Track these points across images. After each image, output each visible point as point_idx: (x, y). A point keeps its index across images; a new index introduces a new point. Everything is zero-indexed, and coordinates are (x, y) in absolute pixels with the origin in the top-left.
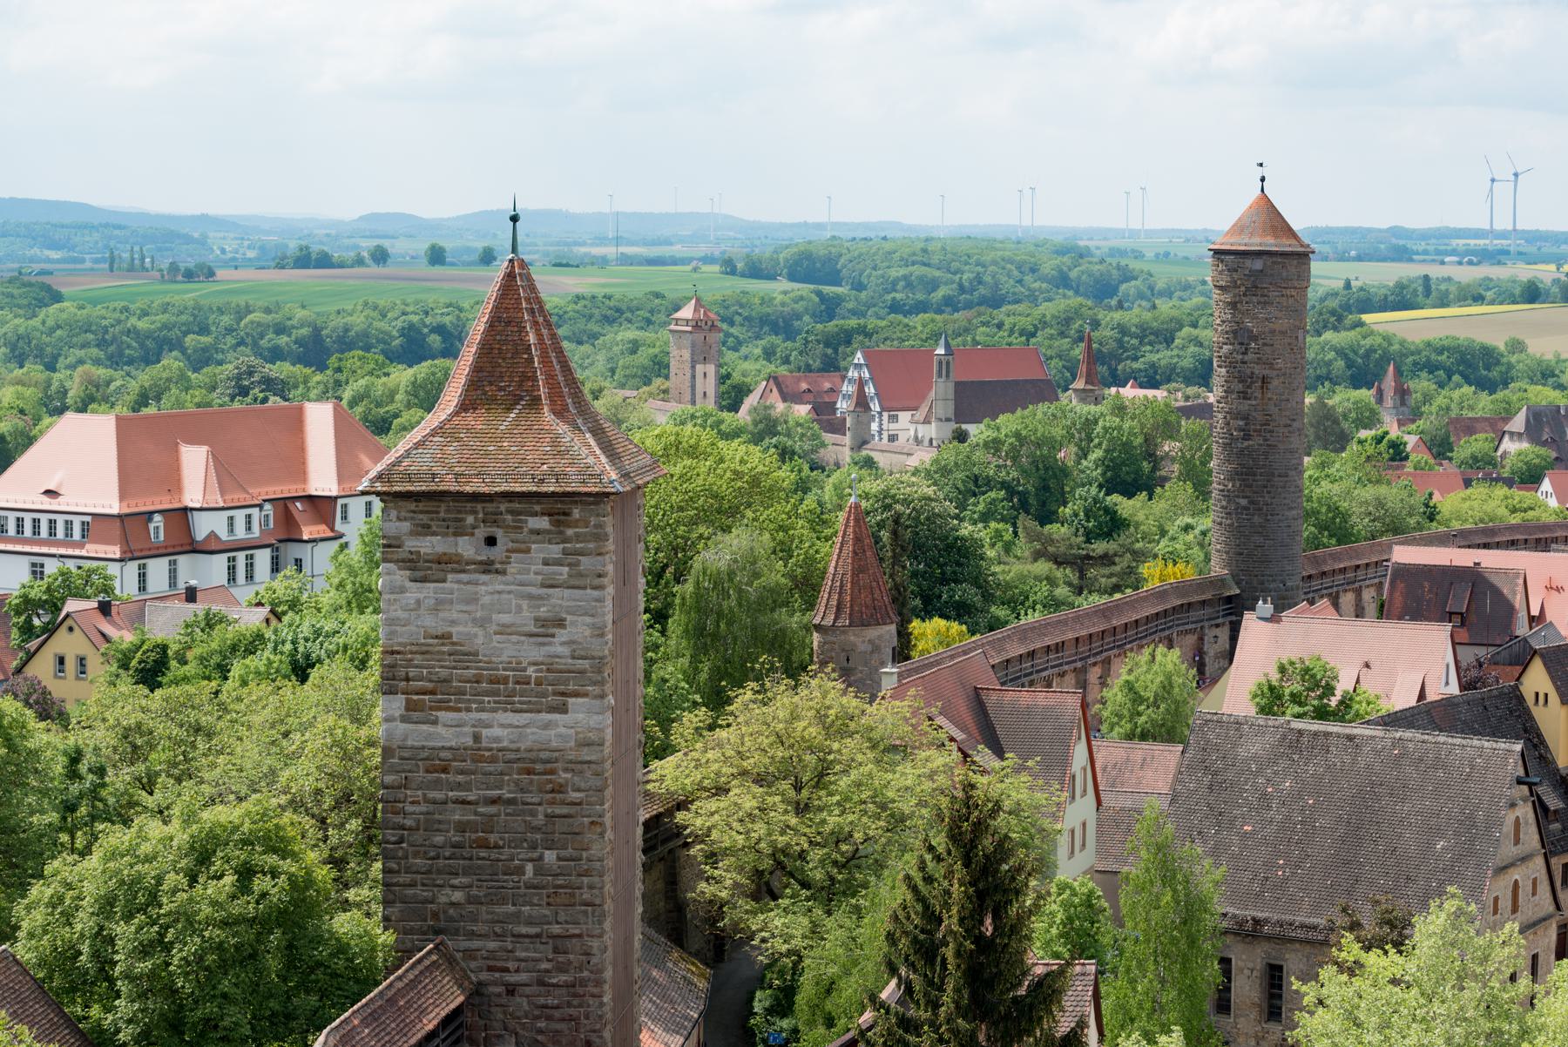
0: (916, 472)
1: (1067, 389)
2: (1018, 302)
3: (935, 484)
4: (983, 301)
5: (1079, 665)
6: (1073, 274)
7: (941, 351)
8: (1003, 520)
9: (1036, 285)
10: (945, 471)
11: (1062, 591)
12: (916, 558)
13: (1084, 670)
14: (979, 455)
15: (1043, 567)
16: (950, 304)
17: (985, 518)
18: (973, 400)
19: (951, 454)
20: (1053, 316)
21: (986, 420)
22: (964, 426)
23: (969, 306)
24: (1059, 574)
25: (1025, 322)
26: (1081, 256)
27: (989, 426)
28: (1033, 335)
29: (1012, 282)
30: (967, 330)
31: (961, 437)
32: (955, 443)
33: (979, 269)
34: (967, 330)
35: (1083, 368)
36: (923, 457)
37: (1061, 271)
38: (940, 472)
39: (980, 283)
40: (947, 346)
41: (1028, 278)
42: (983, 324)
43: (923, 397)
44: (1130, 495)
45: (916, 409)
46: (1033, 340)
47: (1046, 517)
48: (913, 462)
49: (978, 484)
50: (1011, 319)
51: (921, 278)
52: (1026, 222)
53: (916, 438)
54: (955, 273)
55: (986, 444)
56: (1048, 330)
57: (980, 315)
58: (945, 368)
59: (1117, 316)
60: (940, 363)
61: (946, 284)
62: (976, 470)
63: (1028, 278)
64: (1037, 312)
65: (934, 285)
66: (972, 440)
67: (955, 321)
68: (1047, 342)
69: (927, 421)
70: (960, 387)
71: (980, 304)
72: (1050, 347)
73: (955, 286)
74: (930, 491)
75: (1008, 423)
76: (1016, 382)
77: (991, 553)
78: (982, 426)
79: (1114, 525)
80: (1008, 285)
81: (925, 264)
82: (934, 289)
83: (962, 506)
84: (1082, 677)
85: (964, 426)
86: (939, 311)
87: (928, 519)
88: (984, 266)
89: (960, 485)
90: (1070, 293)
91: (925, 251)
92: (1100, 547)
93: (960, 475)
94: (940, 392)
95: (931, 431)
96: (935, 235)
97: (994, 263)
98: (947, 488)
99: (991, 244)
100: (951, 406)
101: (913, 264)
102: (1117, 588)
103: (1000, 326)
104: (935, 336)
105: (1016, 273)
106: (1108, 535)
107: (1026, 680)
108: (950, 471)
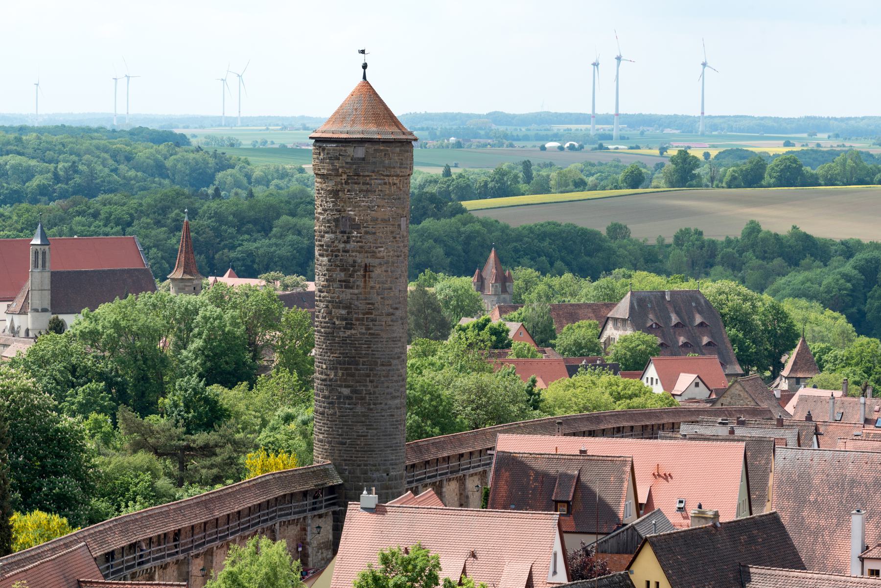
0: (13, 363)
1: (164, 279)
2: (111, 191)
3: (34, 376)
4: (78, 190)
5: (181, 556)
6: (169, 163)
7: (37, 241)
8: (102, 410)
9: (132, 173)
10: (42, 362)
11: (163, 483)
12: (15, 450)
13: (186, 562)
14: (75, 346)
15: (142, 458)
16: (44, 192)
17: (85, 409)
18: (71, 290)
19: (50, 344)
20: (149, 205)
21: (85, 310)
22: (61, 317)
23: (63, 195)
24: (159, 465)
25: (119, 211)
26: (178, 145)
27: (87, 316)
28: (129, 224)
29: (107, 170)
30: (62, 220)
31: (58, 327)
32: (53, 334)
33: (74, 158)
34: (62, 220)
35: (181, 258)
36: (20, 348)
37: (156, 160)
38: (37, 363)
39: (76, 171)
40: (43, 236)
41: (123, 168)
42: (79, 213)
43: (18, 288)
44: (229, 384)
45: (12, 300)
46: (129, 230)
47: (146, 408)
48: (10, 353)
49: (76, 374)
50: (107, 209)
51: (14, 168)
52: (121, 111)
53: (12, 328)
54: (50, 162)
55: (83, 335)
56: (144, 220)
57: (75, 204)
58: (41, 258)
59: (214, 205)
60: (36, 253)
61: (41, 173)
62: (74, 360)
63: (123, 168)
64: (133, 202)
65: (29, 174)
66: (69, 331)
67: (50, 211)
68: (143, 232)
69: (23, 312)
70: (56, 277)
71: (75, 193)
72: (146, 236)
73: (50, 175)
74: (28, 382)
75: (107, 312)
76: (113, 272)
77: (90, 445)
78: (80, 317)
79: (212, 415)
80: (102, 171)
81: (19, 154)
82: (29, 179)
83: (61, 398)
84: (184, 569)
85: (61, 317)
86: (34, 201)
87: (27, 410)
88: (79, 155)
89: (59, 376)
90: (166, 182)
91: (19, 140)
92: (201, 438)
93: (60, 366)
94: (37, 283)
95: (25, 322)
96: (29, 123)
97: (88, 152)
98: (45, 380)
99: (87, 132)
100: (47, 295)
101: (8, 153)
102: (217, 479)
103: (96, 215)
104: (31, 227)
105: (111, 162)
106: (208, 426)
107: (128, 573)
108: (48, 362)
